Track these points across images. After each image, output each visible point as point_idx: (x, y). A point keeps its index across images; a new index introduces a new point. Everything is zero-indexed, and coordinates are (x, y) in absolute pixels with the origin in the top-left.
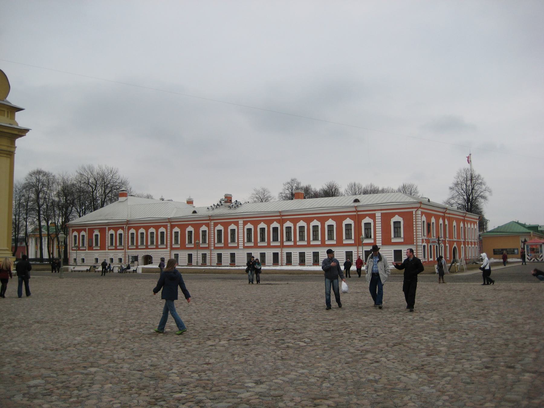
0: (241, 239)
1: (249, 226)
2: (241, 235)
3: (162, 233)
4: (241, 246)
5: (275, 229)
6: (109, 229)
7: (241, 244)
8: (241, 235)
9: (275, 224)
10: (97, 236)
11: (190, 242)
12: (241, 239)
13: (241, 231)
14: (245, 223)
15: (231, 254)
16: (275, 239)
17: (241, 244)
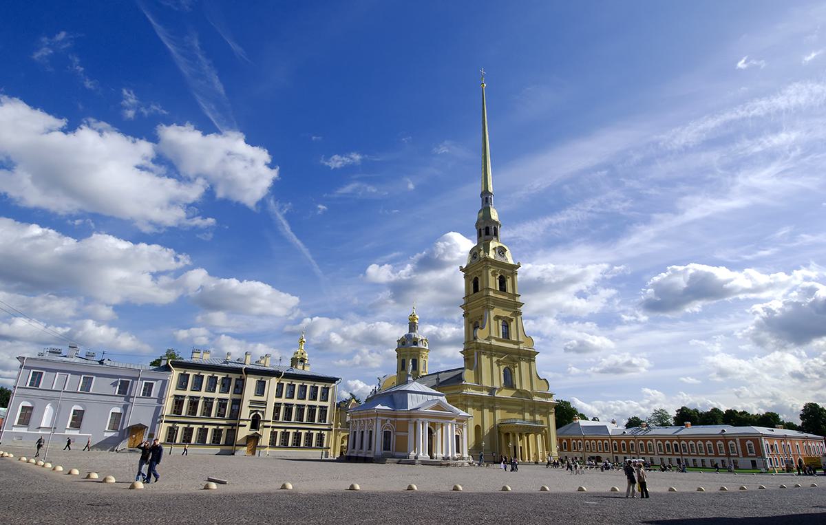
0: (655, 450)
1: (659, 442)
2: (655, 447)
3: (606, 444)
4: (656, 454)
5: (676, 445)
6: (573, 440)
7: (656, 452)
8: (655, 447)
9: (675, 442)
10: (565, 443)
11: (624, 450)
12: (655, 450)
13: (655, 445)
14: (657, 440)
15: (752, 461)
16: (677, 451)
17: (656, 452)
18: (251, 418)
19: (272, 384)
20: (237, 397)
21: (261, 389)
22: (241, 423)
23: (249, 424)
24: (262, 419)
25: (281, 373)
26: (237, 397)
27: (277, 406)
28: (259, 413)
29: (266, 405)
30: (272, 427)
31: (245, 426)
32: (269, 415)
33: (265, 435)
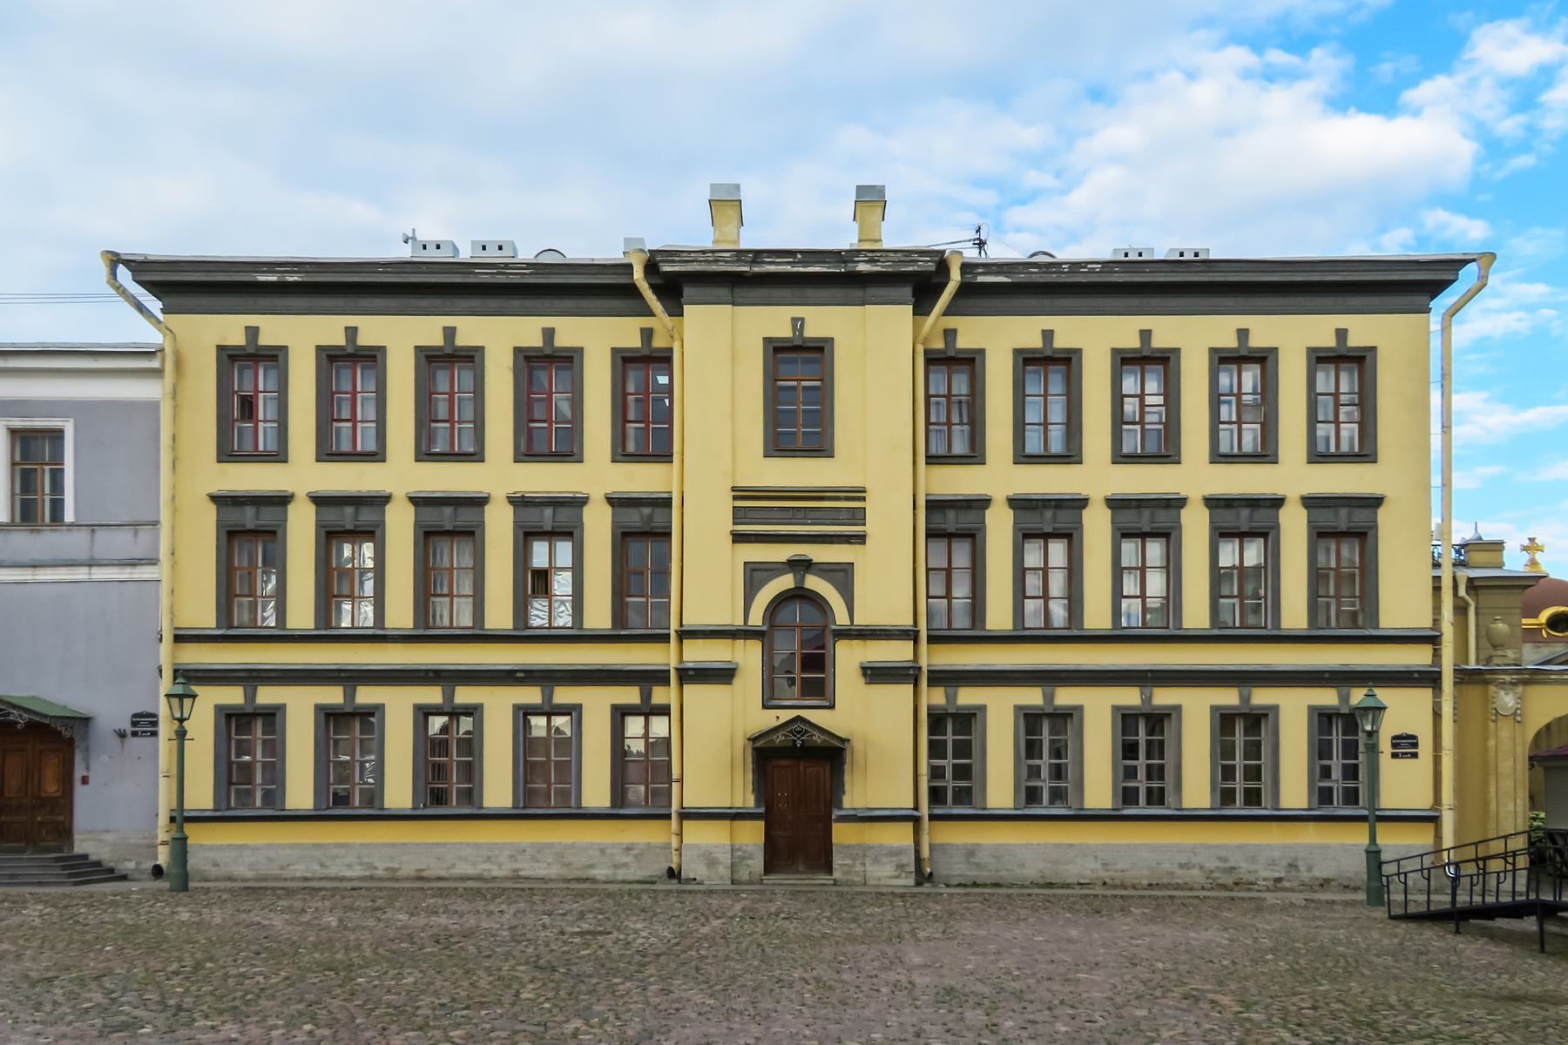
18: (756, 619)
19: (875, 352)
20: (643, 479)
21: (798, 395)
22: (699, 653)
23: (749, 657)
24: (841, 618)
25: (943, 266)
26: (643, 479)
27: (951, 521)
28: (813, 583)
29: (858, 516)
30: (939, 678)
31: (723, 675)
32: (886, 580)
33: (877, 726)
